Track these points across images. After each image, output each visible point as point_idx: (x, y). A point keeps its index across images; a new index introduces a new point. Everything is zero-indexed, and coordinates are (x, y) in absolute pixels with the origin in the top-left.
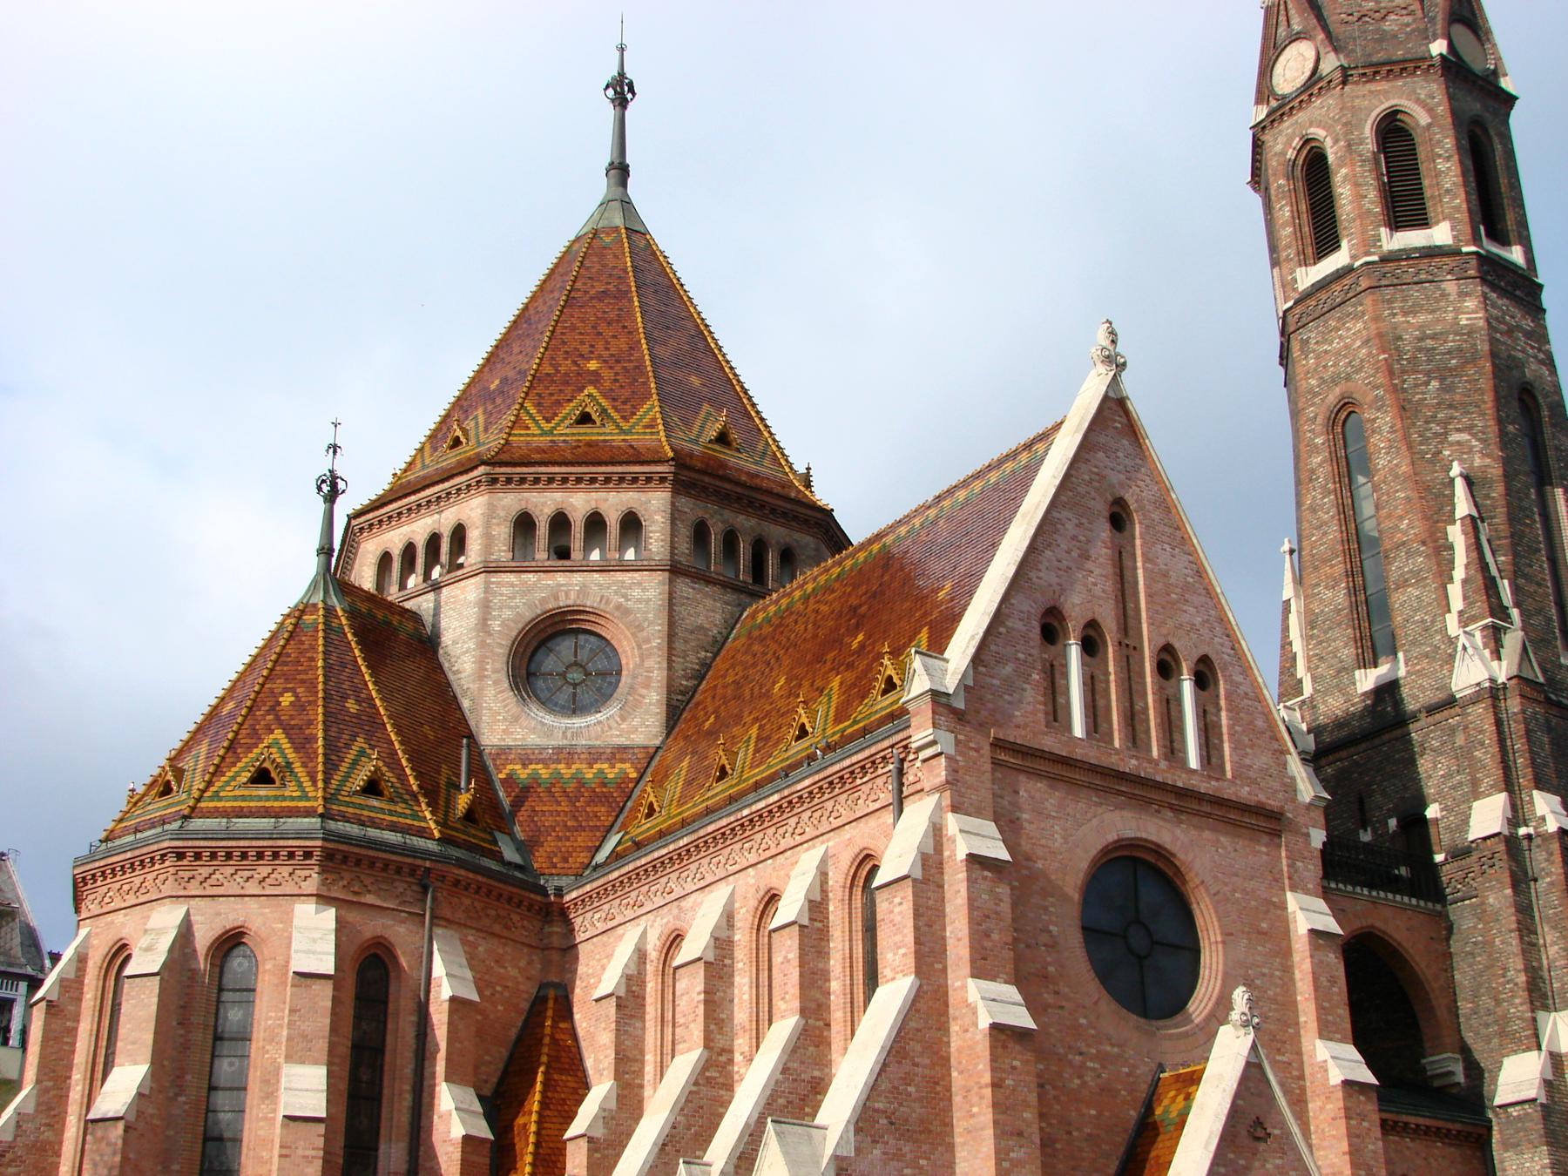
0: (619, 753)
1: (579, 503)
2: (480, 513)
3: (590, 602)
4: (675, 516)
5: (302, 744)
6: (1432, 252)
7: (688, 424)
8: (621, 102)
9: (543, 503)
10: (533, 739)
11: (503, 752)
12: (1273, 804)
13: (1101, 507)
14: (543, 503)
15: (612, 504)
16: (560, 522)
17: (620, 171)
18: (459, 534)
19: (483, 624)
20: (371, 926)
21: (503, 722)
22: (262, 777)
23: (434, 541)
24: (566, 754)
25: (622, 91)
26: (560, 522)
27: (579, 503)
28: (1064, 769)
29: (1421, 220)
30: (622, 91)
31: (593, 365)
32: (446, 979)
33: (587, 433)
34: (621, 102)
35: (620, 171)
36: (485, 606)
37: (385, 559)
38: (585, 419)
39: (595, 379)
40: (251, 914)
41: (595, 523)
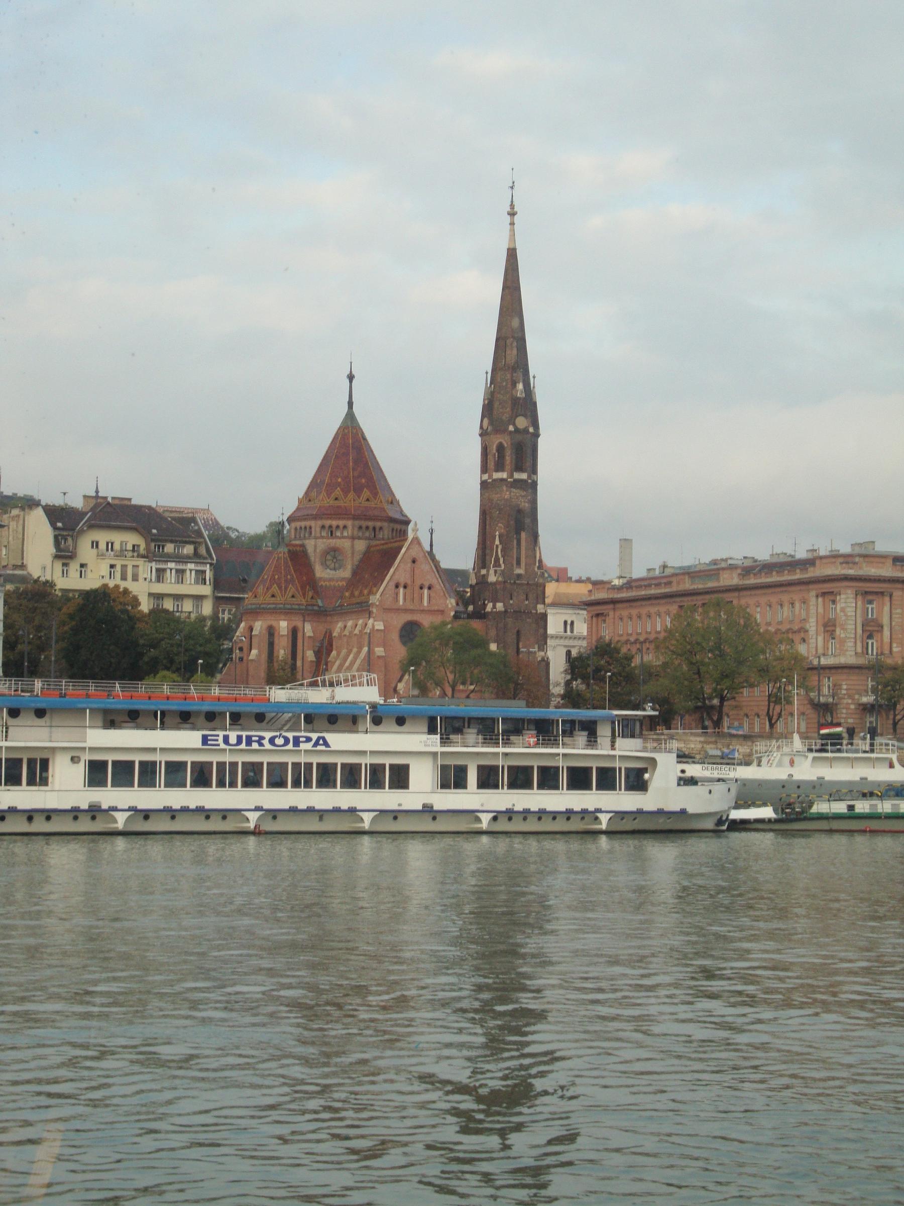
0: (343, 579)
1: (334, 523)
2: (315, 525)
3: (337, 545)
4: (353, 526)
5: (280, 588)
6: (502, 480)
7: (359, 497)
8: (351, 382)
9: (328, 523)
10: (326, 576)
11: (321, 579)
12: (441, 609)
13: (410, 561)
14: (328, 523)
15: (341, 523)
16: (330, 527)
17: (350, 404)
18: (310, 528)
19: (315, 550)
20: (294, 623)
21: (320, 572)
22: (273, 596)
23: (305, 528)
24: (330, 580)
25: (351, 377)
26: (330, 527)
27: (334, 523)
28: (398, 610)
29: (503, 470)
30: (351, 377)
31: (339, 480)
32: (308, 629)
33: (337, 503)
34: (351, 382)
35: (350, 404)
36: (315, 546)
37: (296, 529)
38: (336, 499)
39: (339, 484)
40: (274, 623)
41: (338, 527)
